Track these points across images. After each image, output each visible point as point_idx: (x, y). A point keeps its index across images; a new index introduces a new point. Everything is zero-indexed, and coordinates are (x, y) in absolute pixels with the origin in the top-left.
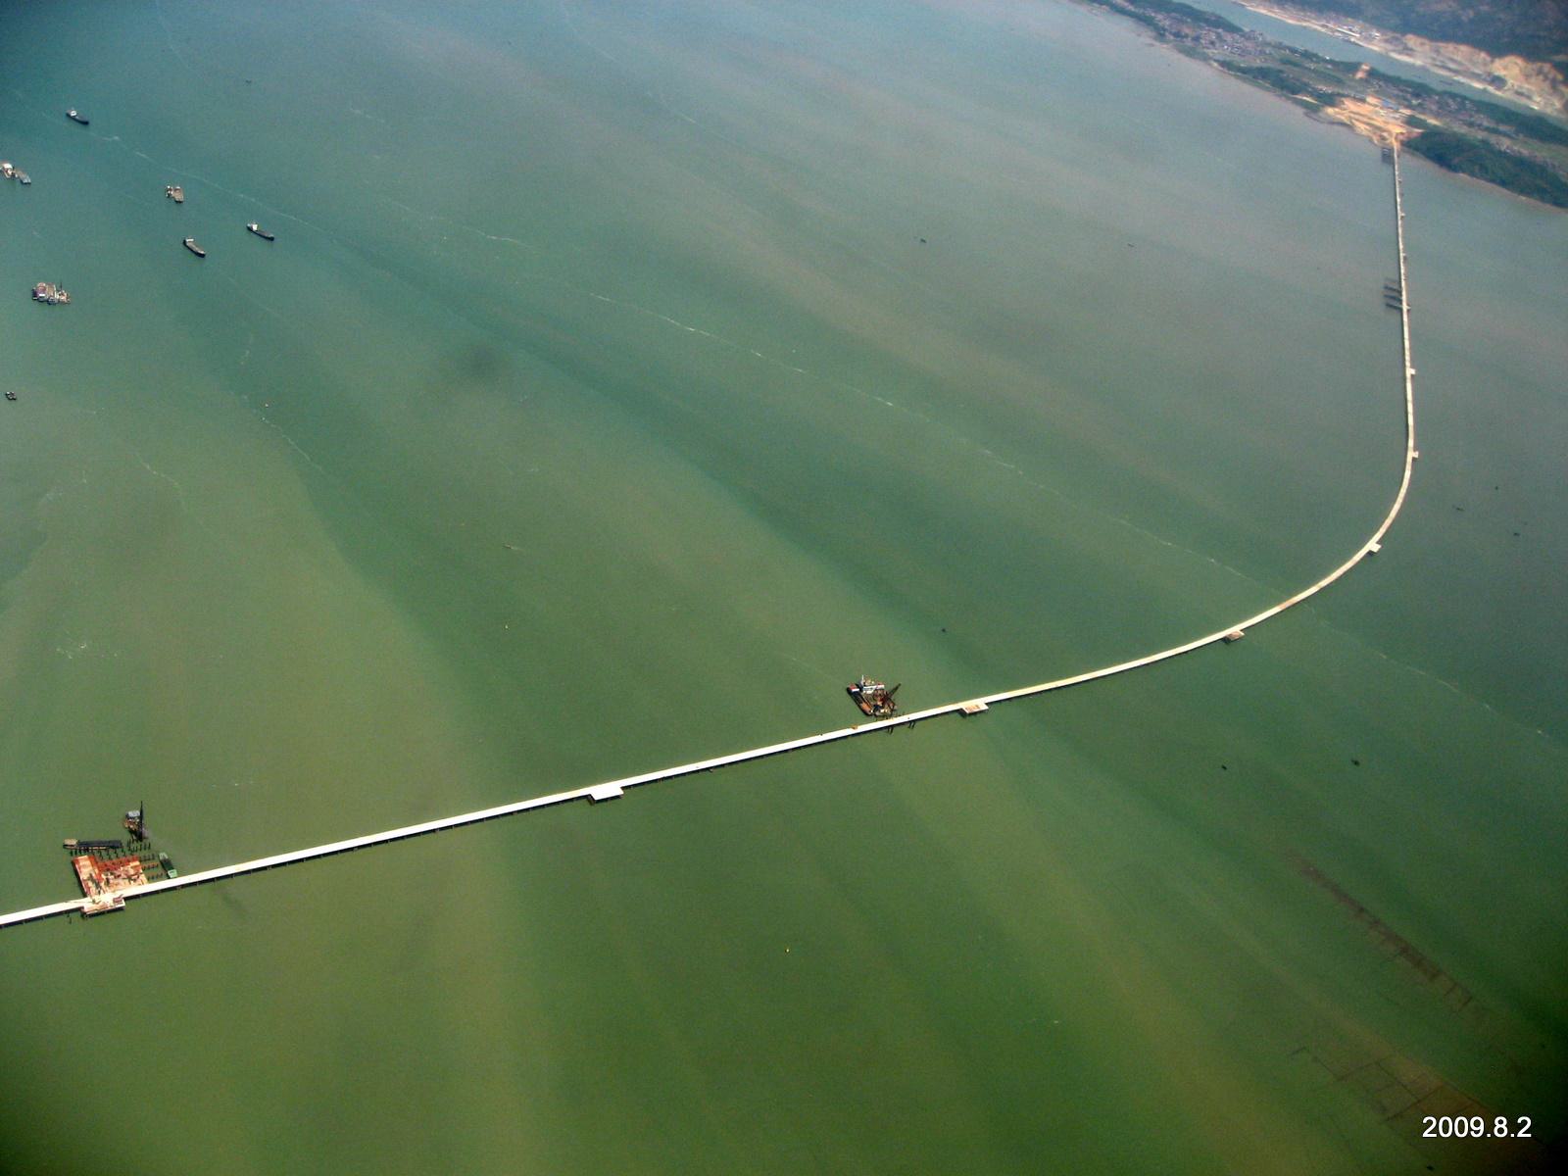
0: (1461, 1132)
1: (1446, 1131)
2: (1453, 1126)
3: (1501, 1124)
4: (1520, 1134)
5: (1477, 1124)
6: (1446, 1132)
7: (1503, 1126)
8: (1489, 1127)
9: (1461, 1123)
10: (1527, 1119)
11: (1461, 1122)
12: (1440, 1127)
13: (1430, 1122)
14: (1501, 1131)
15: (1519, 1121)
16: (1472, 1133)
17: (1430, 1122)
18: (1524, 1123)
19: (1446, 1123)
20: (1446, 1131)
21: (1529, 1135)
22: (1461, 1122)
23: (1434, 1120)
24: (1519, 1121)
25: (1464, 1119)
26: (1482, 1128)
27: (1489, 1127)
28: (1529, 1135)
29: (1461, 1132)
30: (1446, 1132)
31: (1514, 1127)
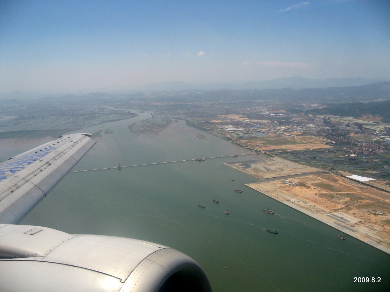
0: (363, 281)
1: (360, 281)
2: (362, 280)
3: (373, 279)
4: (378, 282)
5: (367, 279)
6: (360, 281)
7: (374, 280)
8: (370, 280)
9: (363, 279)
10: (380, 278)
11: (363, 279)
12: (358, 280)
13: (356, 279)
14: (373, 281)
15: (378, 278)
16: (366, 281)
17: (356, 279)
18: (379, 279)
19: (360, 279)
20: (360, 281)
21: (380, 282)
22: (363, 279)
23: (357, 278)
24: (378, 278)
25: (364, 278)
26: (368, 280)
27: (370, 280)
28: (380, 282)
29: (363, 281)
30: (360, 281)
31: (377, 280)
